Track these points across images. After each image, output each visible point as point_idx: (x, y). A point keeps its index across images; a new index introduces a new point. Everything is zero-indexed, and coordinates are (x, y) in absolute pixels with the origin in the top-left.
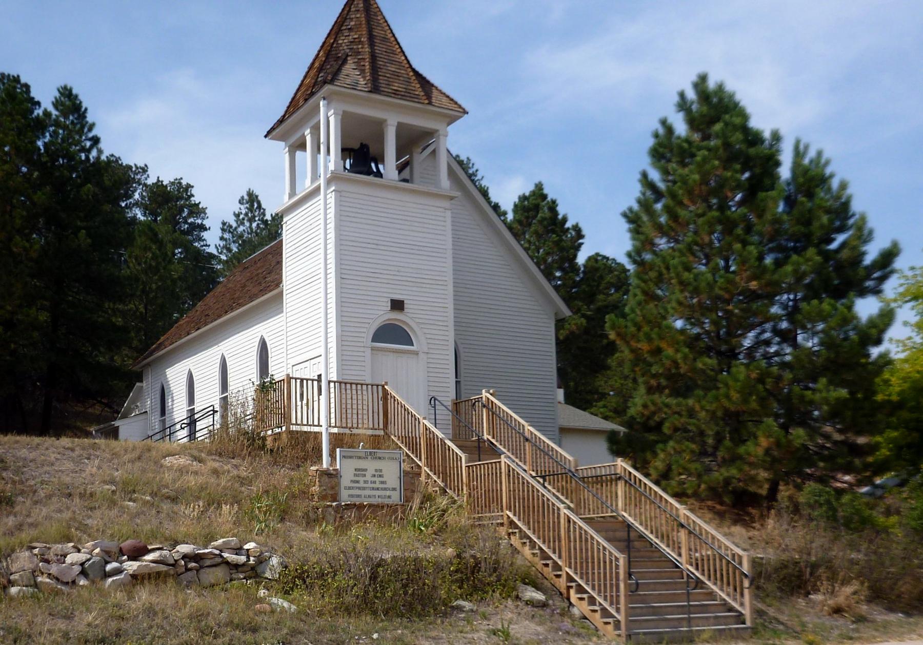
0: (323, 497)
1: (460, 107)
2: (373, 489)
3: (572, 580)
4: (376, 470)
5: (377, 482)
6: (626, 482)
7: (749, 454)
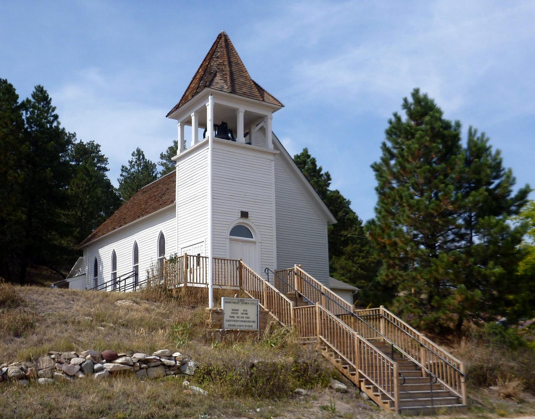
0: (214, 326)
1: (280, 103)
2: (242, 321)
3: (363, 377)
4: (244, 311)
5: (245, 318)
6: (385, 319)
7: (450, 304)
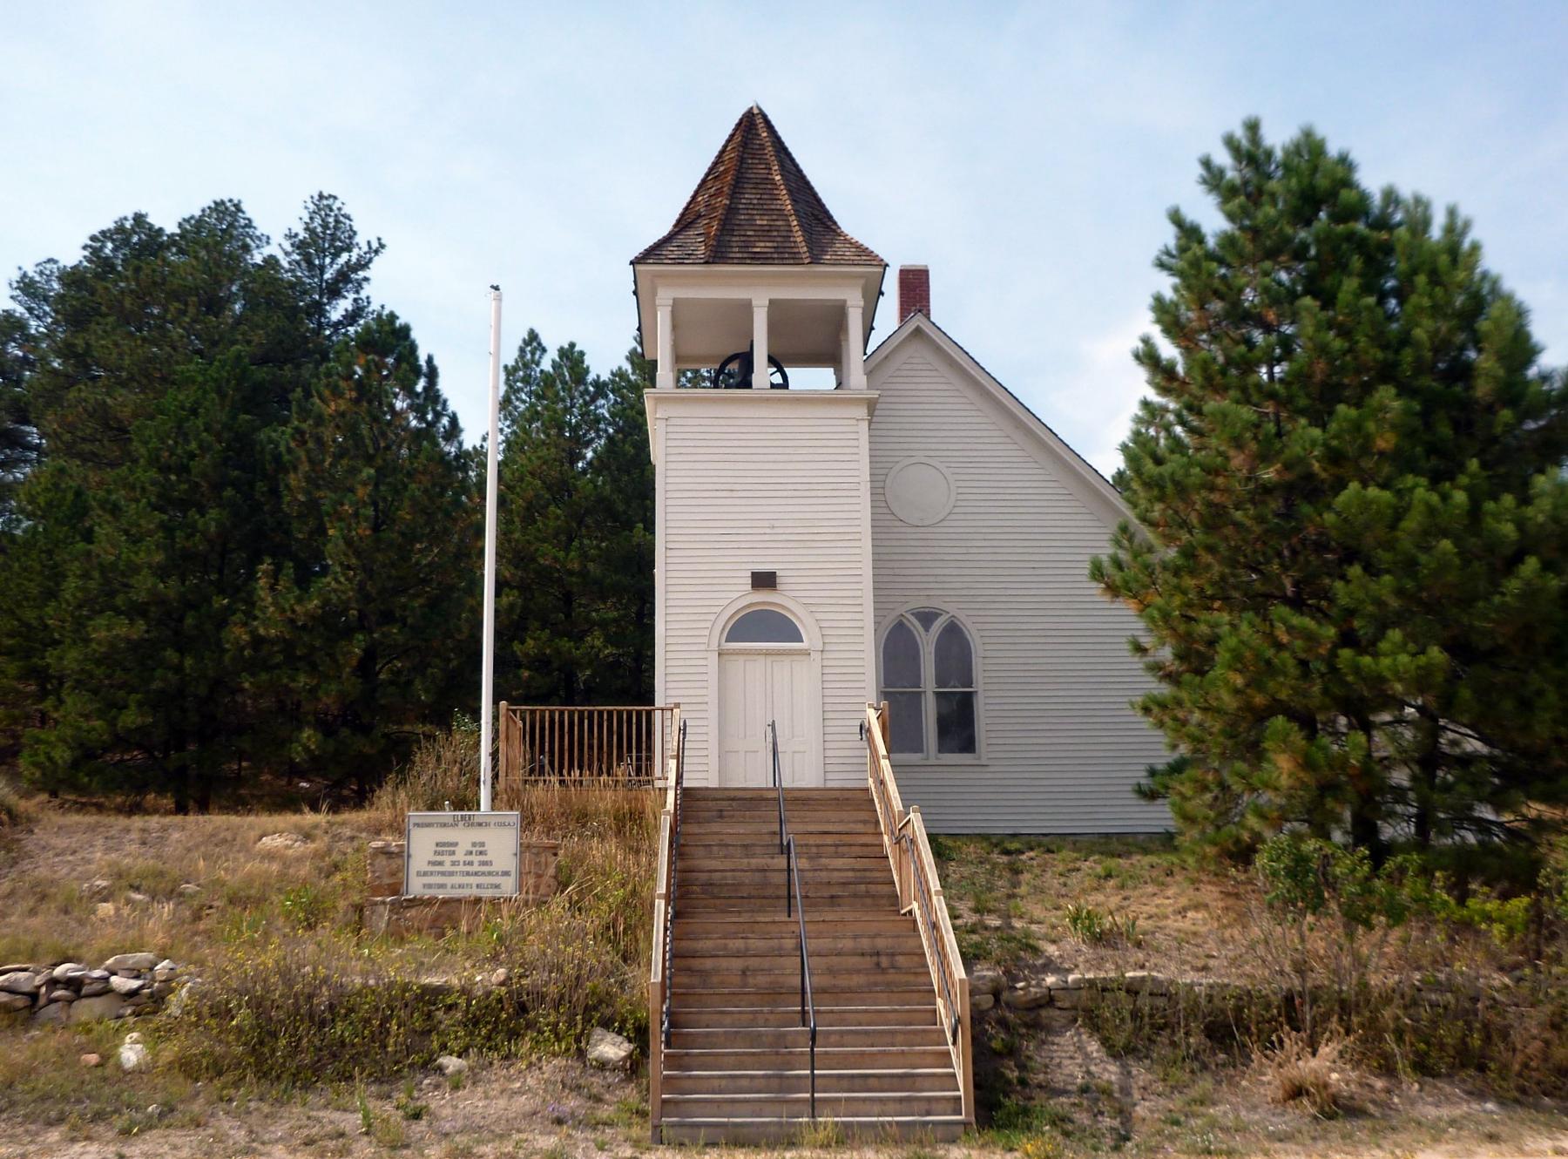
2: (468, 874)
4: (474, 844)
5: (476, 864)
